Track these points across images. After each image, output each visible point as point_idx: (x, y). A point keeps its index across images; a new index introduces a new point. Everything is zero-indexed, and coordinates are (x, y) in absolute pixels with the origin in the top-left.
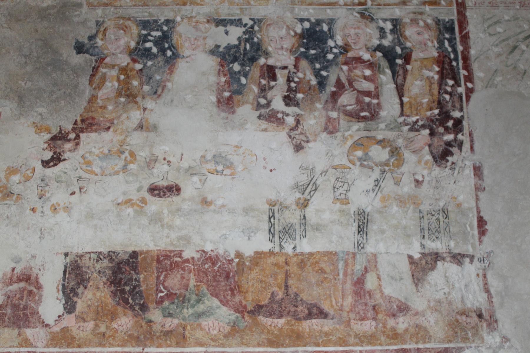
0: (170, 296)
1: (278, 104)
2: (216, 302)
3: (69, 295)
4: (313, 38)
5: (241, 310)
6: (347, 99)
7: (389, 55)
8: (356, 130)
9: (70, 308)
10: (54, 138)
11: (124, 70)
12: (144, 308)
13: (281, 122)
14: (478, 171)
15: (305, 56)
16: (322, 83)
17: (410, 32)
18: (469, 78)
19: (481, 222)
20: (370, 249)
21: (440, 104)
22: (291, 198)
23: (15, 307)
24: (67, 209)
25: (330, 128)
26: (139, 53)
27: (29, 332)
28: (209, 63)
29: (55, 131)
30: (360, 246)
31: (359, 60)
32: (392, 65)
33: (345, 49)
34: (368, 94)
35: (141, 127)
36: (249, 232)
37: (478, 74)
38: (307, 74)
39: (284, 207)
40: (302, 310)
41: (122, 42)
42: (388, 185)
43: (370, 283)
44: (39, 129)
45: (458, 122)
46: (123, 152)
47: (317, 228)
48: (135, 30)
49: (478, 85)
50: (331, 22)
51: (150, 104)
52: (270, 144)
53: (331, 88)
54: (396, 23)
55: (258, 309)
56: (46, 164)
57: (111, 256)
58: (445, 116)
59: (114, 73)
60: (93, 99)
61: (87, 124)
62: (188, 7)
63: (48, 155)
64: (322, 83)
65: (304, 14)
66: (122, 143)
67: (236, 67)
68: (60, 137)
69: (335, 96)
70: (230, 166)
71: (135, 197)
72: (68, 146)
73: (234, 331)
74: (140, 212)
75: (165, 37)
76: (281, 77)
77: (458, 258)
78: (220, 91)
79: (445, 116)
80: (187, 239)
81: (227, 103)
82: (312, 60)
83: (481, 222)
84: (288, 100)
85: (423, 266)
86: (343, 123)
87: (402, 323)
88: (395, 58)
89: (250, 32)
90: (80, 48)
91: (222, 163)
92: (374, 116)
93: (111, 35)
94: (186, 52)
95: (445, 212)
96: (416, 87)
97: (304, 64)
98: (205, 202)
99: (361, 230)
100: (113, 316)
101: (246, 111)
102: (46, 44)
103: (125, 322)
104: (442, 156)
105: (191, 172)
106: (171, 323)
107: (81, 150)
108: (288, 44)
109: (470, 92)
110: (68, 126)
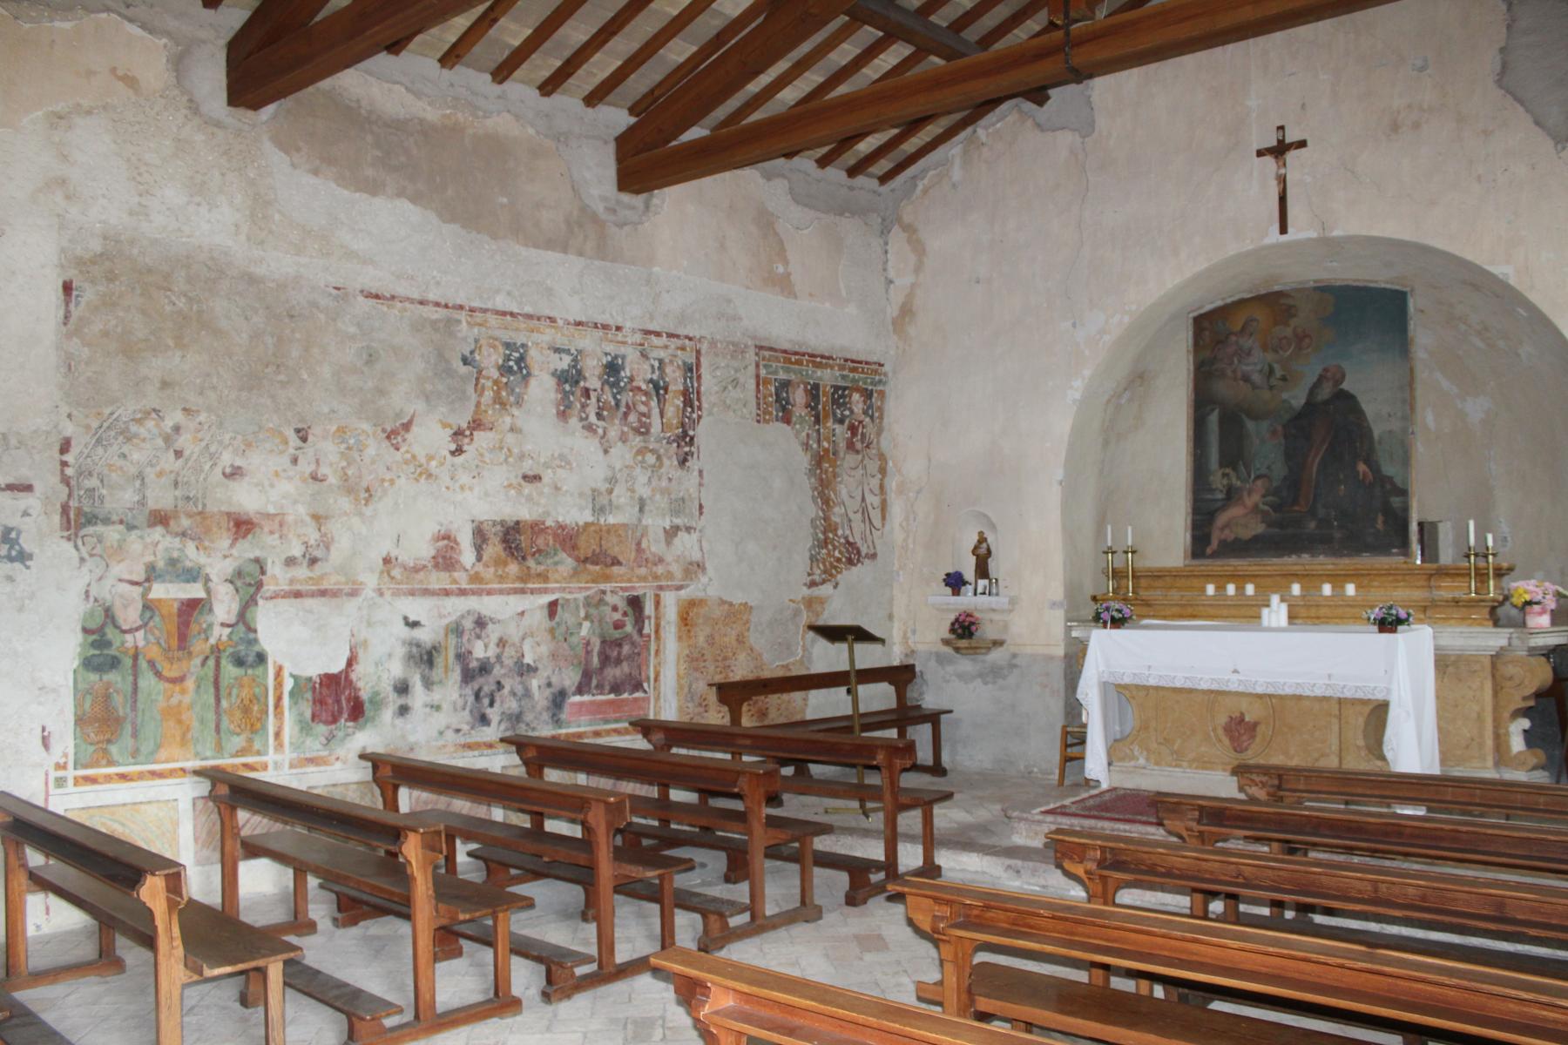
0: (539, 551)
1: (593, 419)
2: (564, 555)
3: (479, 550)
4: (612, 368)
5: (578, 559)
6: (632, 418)
7: (657, 387)
8: (637, 441)
9: (479, 559)
10: (455, 434)
11: (496, 382)
12: (524, 558)
13: (595, 432)
14: (701, 472)
15: (607, 382)
16: (617, 405)
17: (668, 370)
18: (700, 408)
19: (701, 507)
20: (644, 522)
21: (683, 425)
22: (603, 487)
23: (444, 558)
24: (471, 489)
25: (623, 439)
26: (505, 370)
27: (456, 574)
28: (551, 382)
29: (455, 428)
30: (640, 520)
31: (639, 389)
32: (658, 394)
33: (631, 379)
34: (644, 415)
35: (512, 430)
36: (581, 509)
37: (705, 405)
38: (608, 396)
39: (600, 494)
40: (609, 560)
41: (494, 358)
42: (655, 482)
43: (644, 545)
44: (445, 425)
45: (692, 438)
46: (501, 448)
47: (617, 508)
48: (501, 349)
49: (704, 413)
50: (624, 357)
51: (515, 411)
52: (587, 447)
53: (623, 409)
54: (661, 361)
55: (586, 560)
56: (453, 453)
57: (502, 523)
58: (685, 434)
59: (489, 384)
60: (478, 404)
61: (477, 425)
62: (535, 334)
63: (453, 447)
64: (617, 405)
65: (608, 350)
66: (501, 441)
67: (567, 387)
68: (458, 433)
69: (626, 415)
70: (569, 463)
71: (514, 482)
72: (466, 440)
73: (575, 574)
74: (519, 492)
75: (521, 359)
76: (593, 395)
77: (688, 529)
78: (558, 405)
79: (685, 434)
80: (548, 513)
81: (563, 415)
82: (612, 385)
83: (701, 507)
84: (599, 416)
85: (671, 533)
86: (631, 435)
87: (660, 570)
88: (659, 389)
89: (575, 360)
90: (465, 361)
91: (564, 461)
92: (647, 432)
93: (485, 351)
94: (535, 372)
95: (683, 500)
96: (670, 411)
97: (607, 388)
98: (557, 488)
99: (641, 510)
100: (505, 564)
101: (574, 422)
102: (441, 356)
103: (513, 568)
104: (683, 462)
105: (547, 465)
106: (541, 568)
107: (475, 444)
108: (598, 371)
109: (700, 417)
110: (464, 425)
